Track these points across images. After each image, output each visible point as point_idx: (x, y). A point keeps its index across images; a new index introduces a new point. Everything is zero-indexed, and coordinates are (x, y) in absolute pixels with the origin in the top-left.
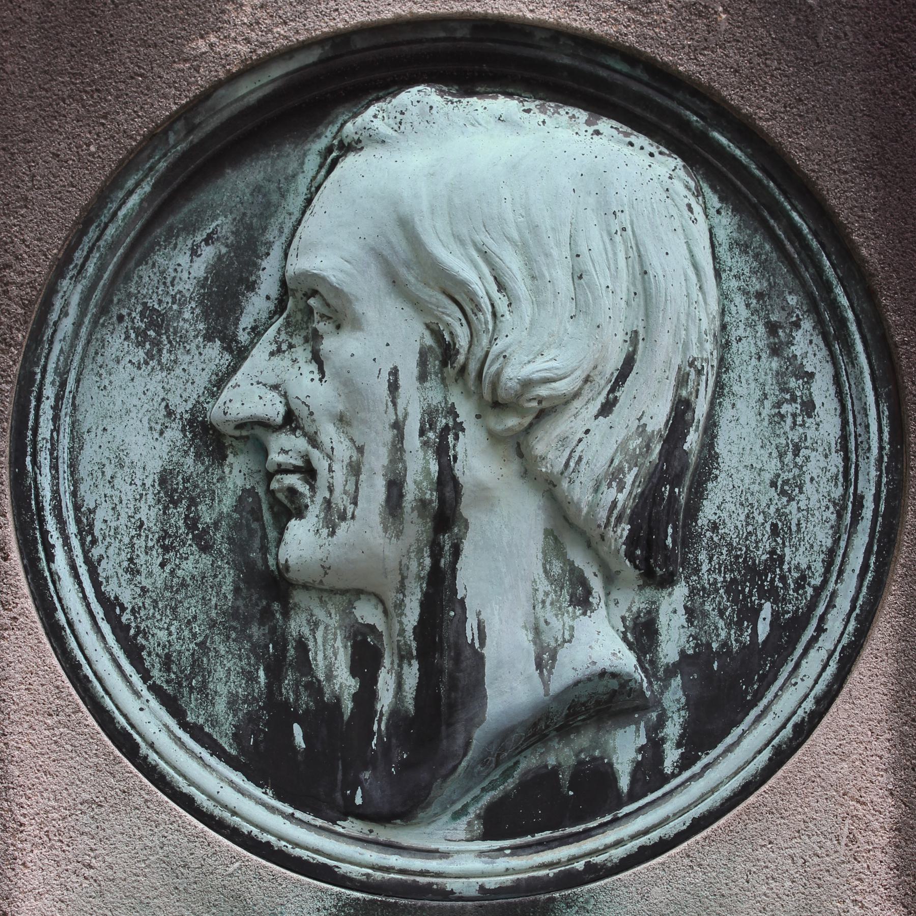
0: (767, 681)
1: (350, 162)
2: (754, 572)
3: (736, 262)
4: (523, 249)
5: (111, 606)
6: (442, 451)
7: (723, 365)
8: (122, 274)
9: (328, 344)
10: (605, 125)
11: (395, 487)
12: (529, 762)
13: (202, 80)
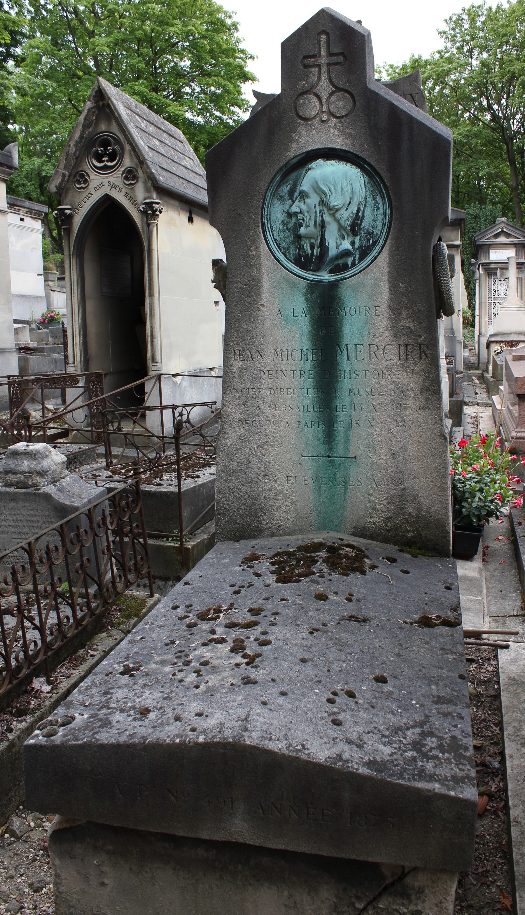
0: (371, 250)
1: (309, 172)
2: (370, 234)
3: (368, 186)
4: (334, 186)
5: (275, 240)
6: (322, 217)
7: (366, 202)
8: (276, 190)
9: (306, 200)
10: (348, 164)
11: (315, 222)
12: (336, 263)
13: (287, 160)
